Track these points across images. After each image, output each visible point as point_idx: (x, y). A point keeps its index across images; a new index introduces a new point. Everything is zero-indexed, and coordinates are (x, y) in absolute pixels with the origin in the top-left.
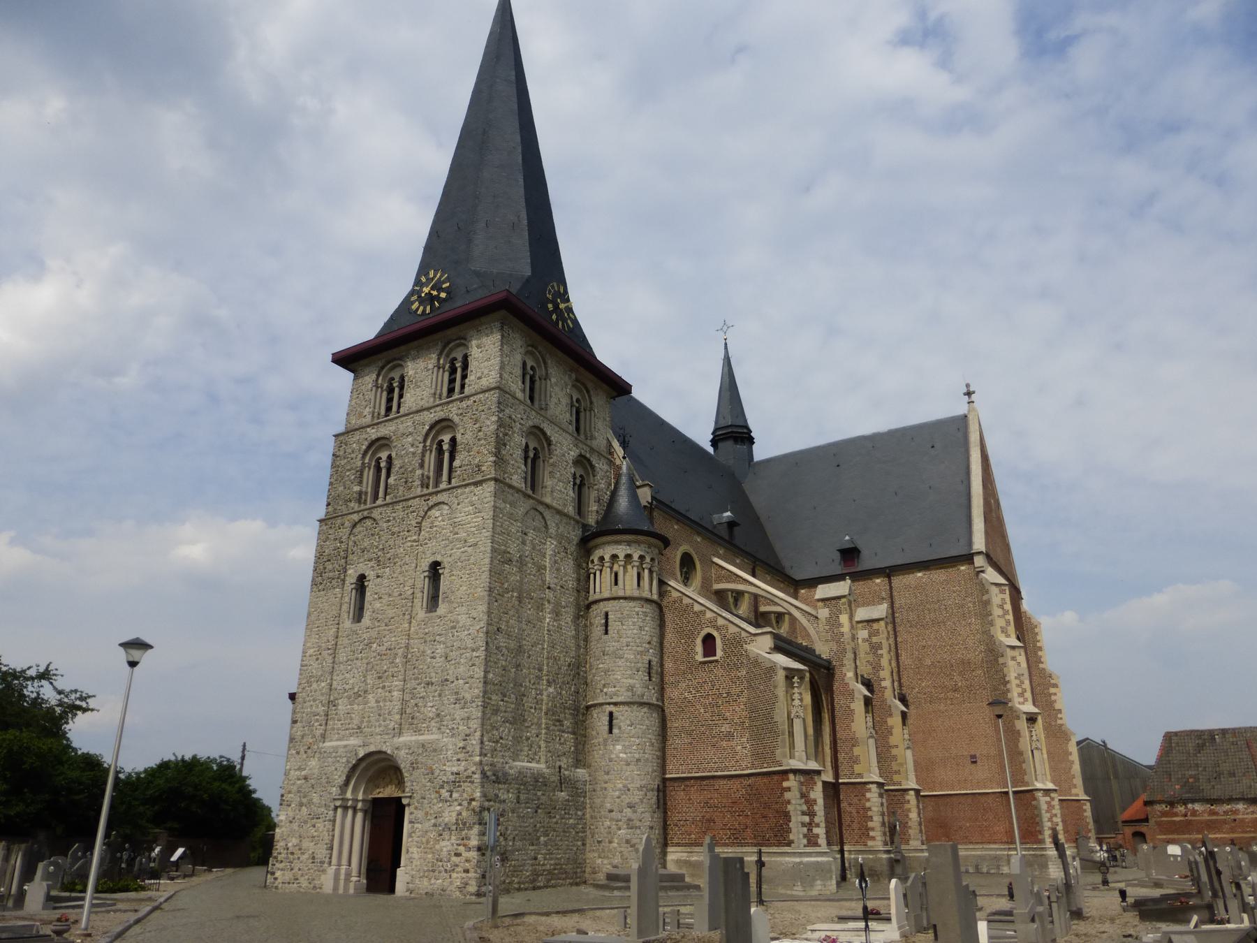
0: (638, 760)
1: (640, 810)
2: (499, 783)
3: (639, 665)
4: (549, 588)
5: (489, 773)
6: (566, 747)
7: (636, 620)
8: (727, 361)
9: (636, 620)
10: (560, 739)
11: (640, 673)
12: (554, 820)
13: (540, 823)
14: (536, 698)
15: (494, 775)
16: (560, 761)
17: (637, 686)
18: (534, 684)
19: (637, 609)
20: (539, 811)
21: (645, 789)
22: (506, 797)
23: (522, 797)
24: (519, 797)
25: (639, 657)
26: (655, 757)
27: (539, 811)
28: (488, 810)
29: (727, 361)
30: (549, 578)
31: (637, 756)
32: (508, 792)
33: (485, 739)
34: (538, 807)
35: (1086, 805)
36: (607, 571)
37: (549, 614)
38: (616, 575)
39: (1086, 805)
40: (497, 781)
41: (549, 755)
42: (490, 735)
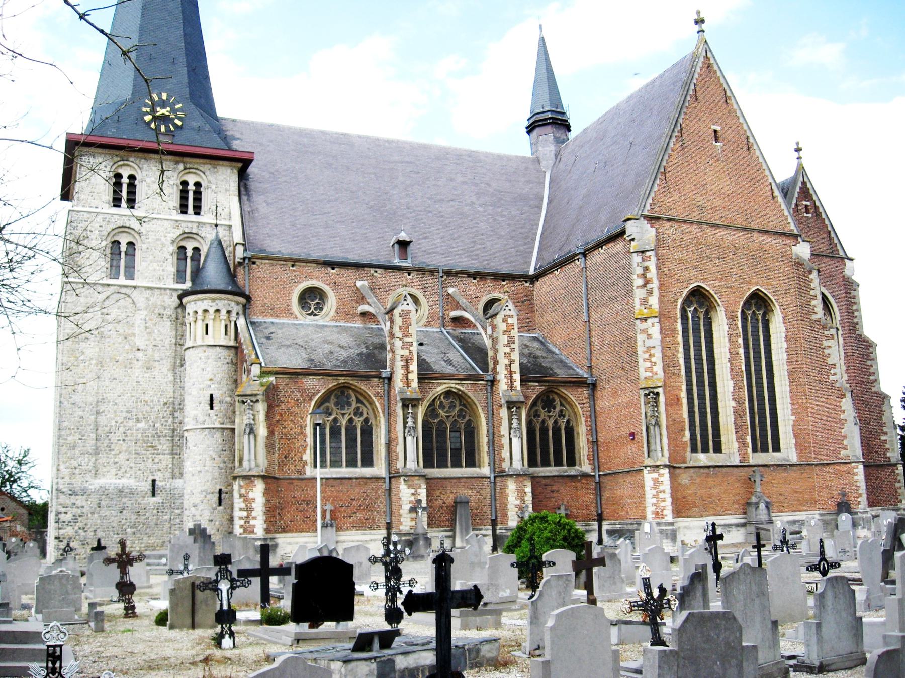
0: (200, 472)
1: (200, 509)
2: (77, 495)
3: (201, 399)
4: (139, 349)
5: (64, 490)
6: (162, 466)
7: (198, 364)
8: (542, 40)
9: (198, 364)
10: (153, 460)
11: (202, 405)
12: (145, 517)
13: (126, 519)
14: (124, 433)
15: (71, 490)
16: (153, 475)
17: (200, 415)
18: (121, 423)
19: (200, 355)
20: (125, 512)
21: (204, 493)
22: (84, 503)
23: (103, 503)
24: (99, 503)
25: (201, 392)
26: (217, 468)
27: (125, 512)
28: (66, 513)
29: (542, 40)
30: (140, 343)
31: (199, 469)
32: (87, 500)
33: (62, 467)
34: (124, 509)
35: (857, 467)
36: (199, 323)
37: (138, 368)
38: (207, 326)
39: (857, 467)
40: (74, 493)
41: (139, 472)
42: (68, 464)
